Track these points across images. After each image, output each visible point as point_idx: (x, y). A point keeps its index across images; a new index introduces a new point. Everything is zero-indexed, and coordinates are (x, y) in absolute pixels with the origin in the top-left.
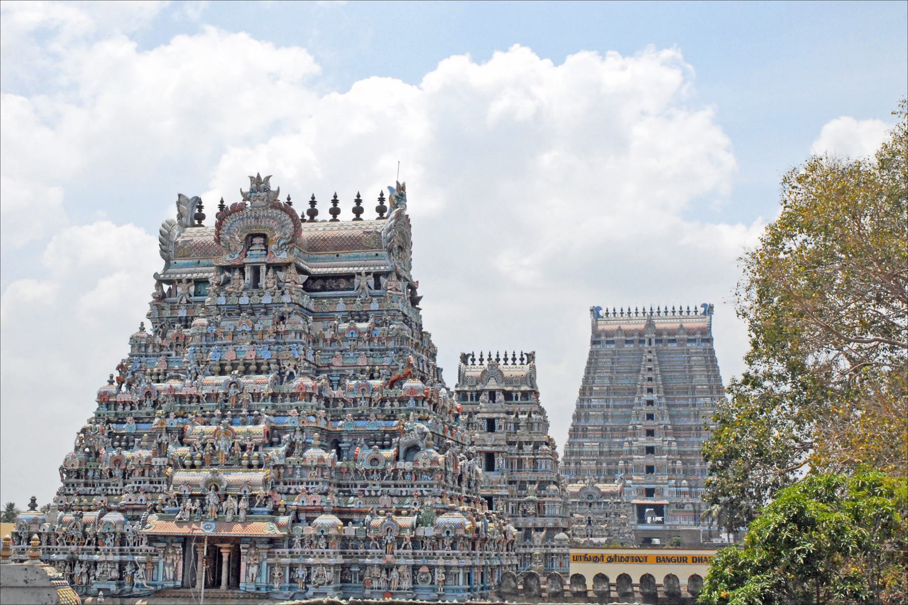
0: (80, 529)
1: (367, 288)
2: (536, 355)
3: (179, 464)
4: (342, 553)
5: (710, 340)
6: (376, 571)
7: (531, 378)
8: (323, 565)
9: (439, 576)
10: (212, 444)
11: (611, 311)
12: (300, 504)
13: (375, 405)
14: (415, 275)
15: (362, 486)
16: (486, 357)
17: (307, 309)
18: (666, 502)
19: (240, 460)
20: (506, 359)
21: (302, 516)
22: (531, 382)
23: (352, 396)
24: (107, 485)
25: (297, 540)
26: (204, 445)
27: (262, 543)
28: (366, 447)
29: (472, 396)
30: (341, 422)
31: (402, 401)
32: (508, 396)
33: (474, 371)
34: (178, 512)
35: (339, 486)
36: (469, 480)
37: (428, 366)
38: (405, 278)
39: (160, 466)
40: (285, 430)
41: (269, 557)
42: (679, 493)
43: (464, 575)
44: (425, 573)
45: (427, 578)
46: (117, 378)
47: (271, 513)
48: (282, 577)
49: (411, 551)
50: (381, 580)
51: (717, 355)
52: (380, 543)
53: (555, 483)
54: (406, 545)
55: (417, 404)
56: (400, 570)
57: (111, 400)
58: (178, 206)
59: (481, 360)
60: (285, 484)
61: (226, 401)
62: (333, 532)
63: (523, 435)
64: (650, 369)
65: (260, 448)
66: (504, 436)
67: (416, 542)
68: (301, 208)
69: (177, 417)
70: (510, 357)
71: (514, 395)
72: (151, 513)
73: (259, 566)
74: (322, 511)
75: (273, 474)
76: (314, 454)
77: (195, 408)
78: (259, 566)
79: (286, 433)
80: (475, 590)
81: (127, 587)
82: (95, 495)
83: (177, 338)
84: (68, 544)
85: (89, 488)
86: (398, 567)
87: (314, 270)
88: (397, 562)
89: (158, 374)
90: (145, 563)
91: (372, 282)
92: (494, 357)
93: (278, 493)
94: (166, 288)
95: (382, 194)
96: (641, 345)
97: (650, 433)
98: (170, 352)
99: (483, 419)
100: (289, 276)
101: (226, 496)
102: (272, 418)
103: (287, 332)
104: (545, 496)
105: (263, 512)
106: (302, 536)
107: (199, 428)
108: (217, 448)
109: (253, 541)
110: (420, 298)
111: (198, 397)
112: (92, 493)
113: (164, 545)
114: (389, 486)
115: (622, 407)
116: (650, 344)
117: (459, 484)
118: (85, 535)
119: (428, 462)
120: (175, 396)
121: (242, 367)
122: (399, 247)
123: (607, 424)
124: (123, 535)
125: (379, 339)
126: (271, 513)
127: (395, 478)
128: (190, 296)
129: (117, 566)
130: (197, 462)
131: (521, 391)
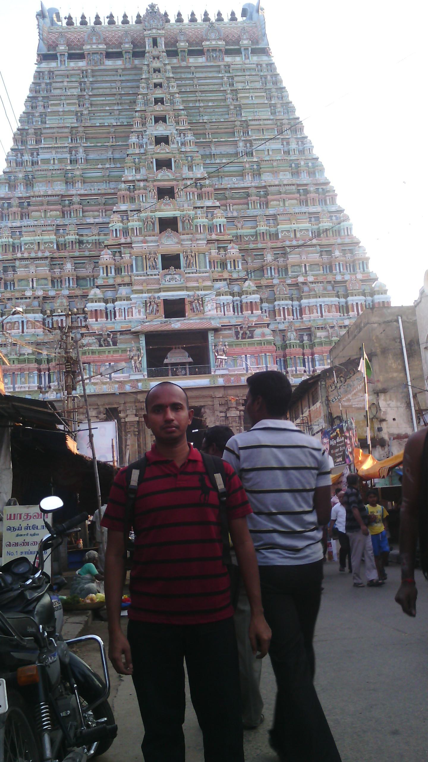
5: (265, 51)
42: (239, 308)
51: (281, 69)
96: (137, 62)
116: (155, 43)
123: (73, 192)
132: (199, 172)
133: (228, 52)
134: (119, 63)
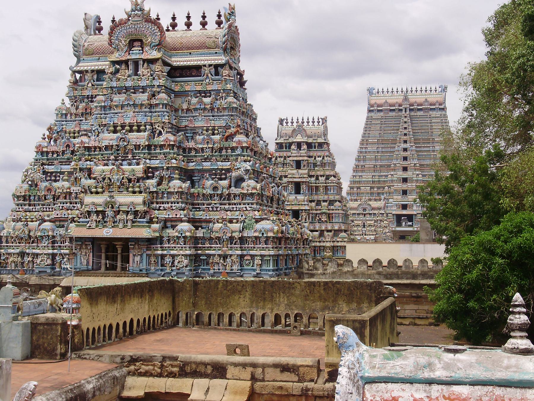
0: (27, 232)
1: (209, 75)
2: (328, 119)
3: (87, 191)
4: (194, 247)
6: (216, 259)
7: (325, 134)
8: (182, 255)
9: (258, 261)
10: (109, 178)
11: (380, 90)
12: (167, 216)
13: (215, 152)
14: (242, 66)
15: (207, 205)
16: (295, 121)
17: (170, 89)
18: (415, 213)
19: (128, 188)
20: (308, 122)
21: (169, 224)
22: (324, 136)
23: (200, 146)
24: (43, 205)
25: (165, 239)
26: (104, 179)
27: (143, 241)
28: (210, 179)
29: (286, 145)
30: (194, 163)
31: (233, 149)
32: (309, 146)
33: (288, 129)
34: (88, 222)
35: (193, 204)
36: (279, 199)
37: (251, 126)
38: (235, 68)
39: (76, 193)
40: (156, 169)
41: (147, 250)
43: (274, 260)
44: (249, 260)
45: (250, 263)
46: (48, 136)
47: (147, 222)
48: (156, 263)
49: (239, 246)
50: (220, 264)
52: (219, 241)
53: (339, 201)
54: (236, 242)
55: (243, 152)
56: (233, 258)
57: (45, 150)
58: (84, 21)
59: (292, 123)
60: (157, 203)
61: (118, 150)
62: (188, 234)
63: (319, 171)
64: (405, 128)
65: (141, 181)
66: (306, 171)
67: (243, 240)
68: (165, 22)
69: (86, 161)
70: (311, 120)
71: (313, 144)
72: (71, 223)
73: (141, 255)
74: (182, 221)
75: (149, 197)
76: (176, 184)
77: (98, 155)
78: (141, 255)
79: (157, 171)
80: (281, 270)
81: (58, 269)
82: (36, 211)
83: (86, 109)
84: (19, 243)
85: (31, 207)
86: (231, 256)
87: (175, 63)
88: (230, 252)
89: (74, 133)
90: (68, 255)
91: (213, 71)
92: (300, 121)
93: (153, 209)
94: (78, 76)
95: (219, 13)
97: (405, 169)
98: (82, 118)
99: (293, 161)
100: (157, 67)
101: (119, 211)
102: (148, 161)
103: (157, 105)
104: (333, 210)
105: (143, 222)
106: (169, 237)
107: (101, 167)
108: (113, 180)
109: (137, 241)
110: (246, 81)
111: (100, 148)
112: (34, 210)
113: (80, 243)
114: (225, 204)
115: (387, 152)
116: (406, 112)
117: (271, 203)
118: (30, 237)
119: (250, 189)
120: (85, 147)
121: (127, 128)
122: (231, 47)
124: (54, 237)
125: (218, 109)
126: (147, 222)
127: (229, 199)
128: (94, 81)
129: (51, 257)
130: (100, 190)
131: (318, 143)
132: (416, 161)
133: (431, 109)
134: (393, 114)
